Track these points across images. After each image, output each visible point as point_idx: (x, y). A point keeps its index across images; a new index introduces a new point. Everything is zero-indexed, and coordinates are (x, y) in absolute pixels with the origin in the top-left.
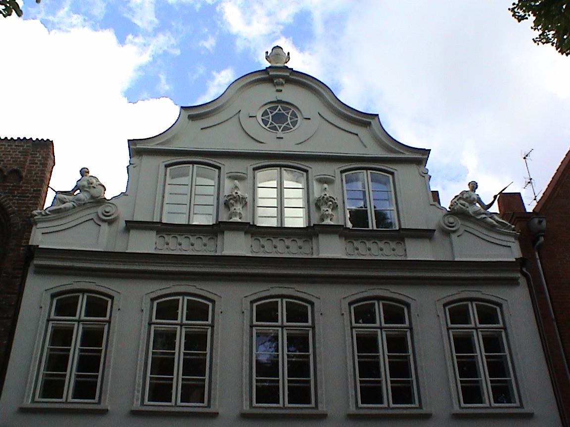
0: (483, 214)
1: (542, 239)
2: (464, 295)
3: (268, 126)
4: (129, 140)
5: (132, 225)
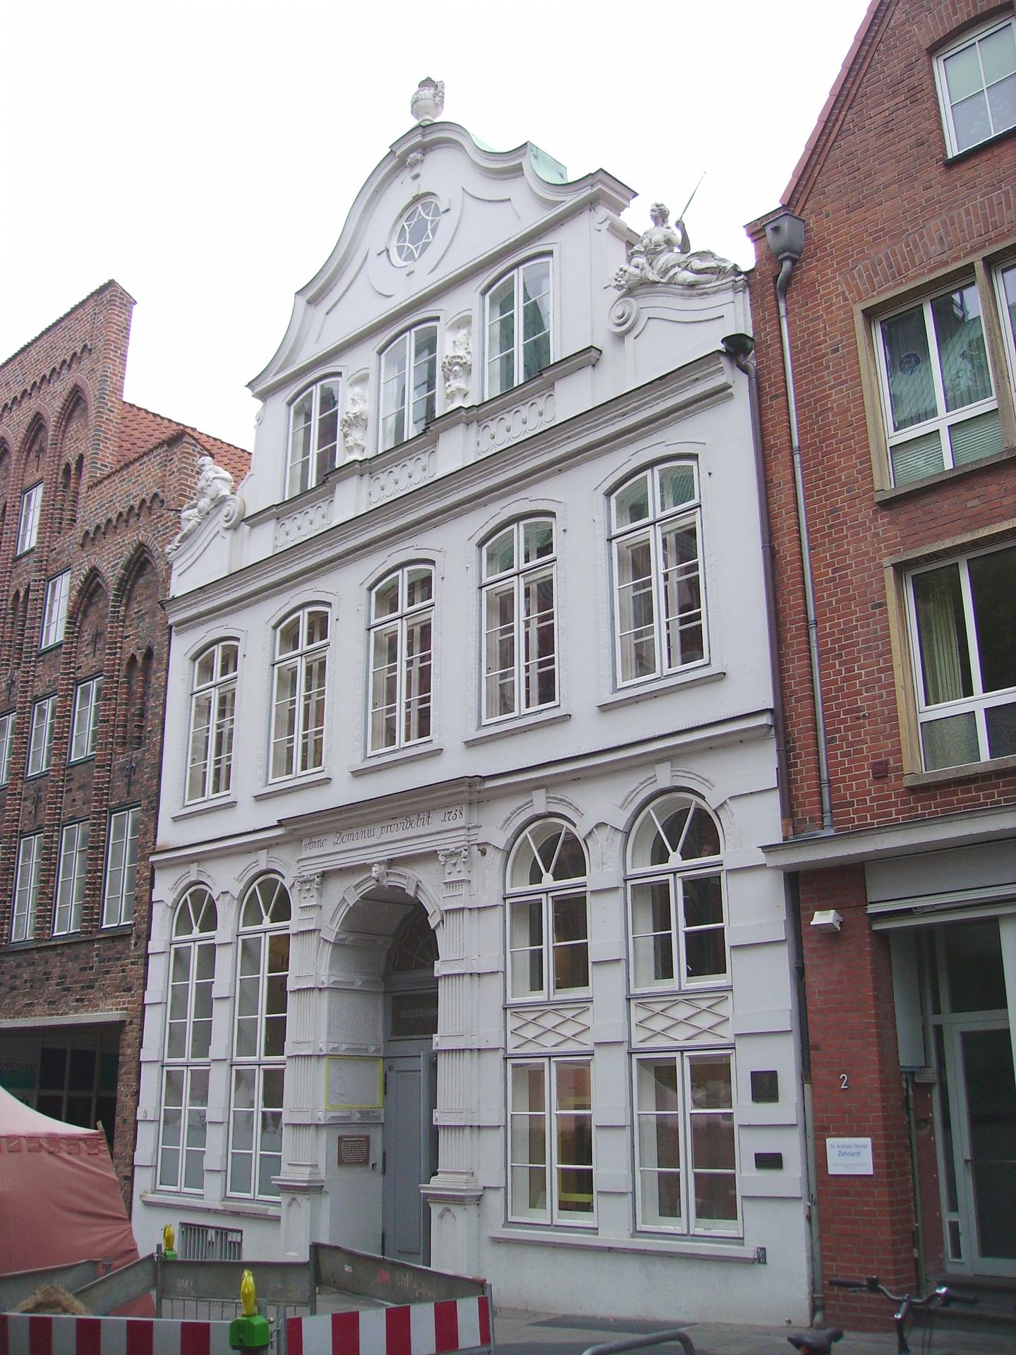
1: (787, 265)
3: (404, 256)
4: (246, 386)
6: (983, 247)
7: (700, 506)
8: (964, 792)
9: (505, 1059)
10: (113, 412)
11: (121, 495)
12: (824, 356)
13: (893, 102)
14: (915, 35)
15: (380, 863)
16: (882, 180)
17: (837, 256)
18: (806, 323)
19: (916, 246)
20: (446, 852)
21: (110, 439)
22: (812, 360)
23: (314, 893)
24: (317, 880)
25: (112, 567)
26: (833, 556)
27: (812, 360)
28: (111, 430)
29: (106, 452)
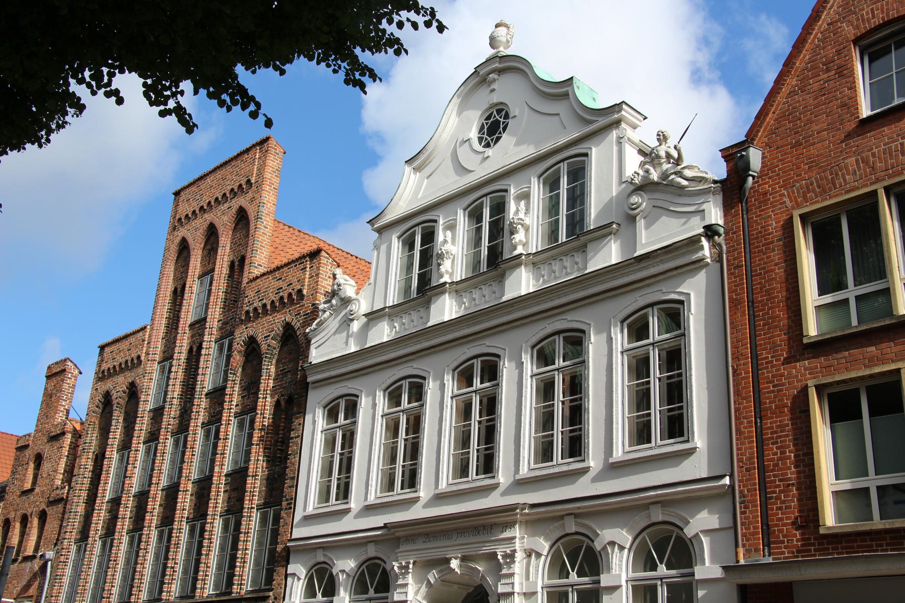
0: (672, 174)
2: (641, 303)
3: (483, 144)
5: (373, 316)
6: (884, 180)
7: (685, 335)
8: (862, 541)
10: (267, 228)
11: (273, 288)
12: (773, 242)
13: (826, 75)
14: (844, 30)
16: (816, 128)
17: (783, 177)
18: (760, 220)
19: (837, 175)
21: (264, 247)
22: (763, 245)
25: (265, 337)
26: (773, 376)
27: (763, 245)
28: (265, 241)
29: (262, 256)
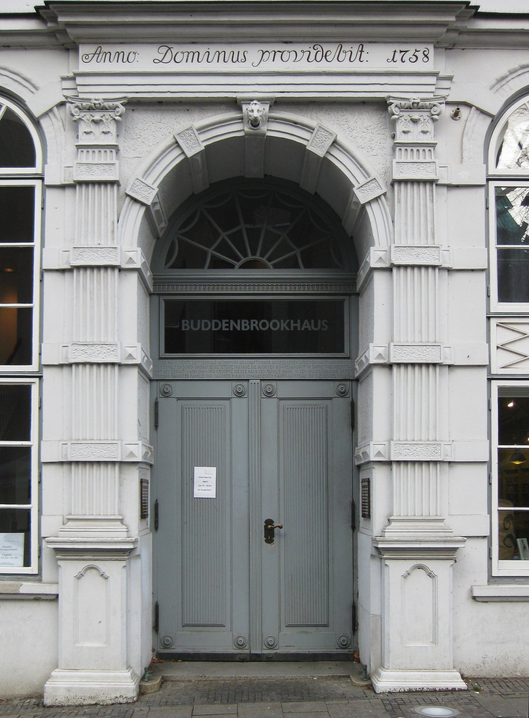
9: (489, 380)
15: (262, 100)
20: (403, 103)
23: (112, 128)
24: (122, 109)
